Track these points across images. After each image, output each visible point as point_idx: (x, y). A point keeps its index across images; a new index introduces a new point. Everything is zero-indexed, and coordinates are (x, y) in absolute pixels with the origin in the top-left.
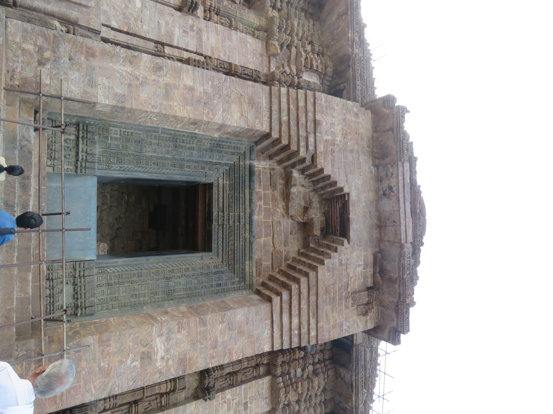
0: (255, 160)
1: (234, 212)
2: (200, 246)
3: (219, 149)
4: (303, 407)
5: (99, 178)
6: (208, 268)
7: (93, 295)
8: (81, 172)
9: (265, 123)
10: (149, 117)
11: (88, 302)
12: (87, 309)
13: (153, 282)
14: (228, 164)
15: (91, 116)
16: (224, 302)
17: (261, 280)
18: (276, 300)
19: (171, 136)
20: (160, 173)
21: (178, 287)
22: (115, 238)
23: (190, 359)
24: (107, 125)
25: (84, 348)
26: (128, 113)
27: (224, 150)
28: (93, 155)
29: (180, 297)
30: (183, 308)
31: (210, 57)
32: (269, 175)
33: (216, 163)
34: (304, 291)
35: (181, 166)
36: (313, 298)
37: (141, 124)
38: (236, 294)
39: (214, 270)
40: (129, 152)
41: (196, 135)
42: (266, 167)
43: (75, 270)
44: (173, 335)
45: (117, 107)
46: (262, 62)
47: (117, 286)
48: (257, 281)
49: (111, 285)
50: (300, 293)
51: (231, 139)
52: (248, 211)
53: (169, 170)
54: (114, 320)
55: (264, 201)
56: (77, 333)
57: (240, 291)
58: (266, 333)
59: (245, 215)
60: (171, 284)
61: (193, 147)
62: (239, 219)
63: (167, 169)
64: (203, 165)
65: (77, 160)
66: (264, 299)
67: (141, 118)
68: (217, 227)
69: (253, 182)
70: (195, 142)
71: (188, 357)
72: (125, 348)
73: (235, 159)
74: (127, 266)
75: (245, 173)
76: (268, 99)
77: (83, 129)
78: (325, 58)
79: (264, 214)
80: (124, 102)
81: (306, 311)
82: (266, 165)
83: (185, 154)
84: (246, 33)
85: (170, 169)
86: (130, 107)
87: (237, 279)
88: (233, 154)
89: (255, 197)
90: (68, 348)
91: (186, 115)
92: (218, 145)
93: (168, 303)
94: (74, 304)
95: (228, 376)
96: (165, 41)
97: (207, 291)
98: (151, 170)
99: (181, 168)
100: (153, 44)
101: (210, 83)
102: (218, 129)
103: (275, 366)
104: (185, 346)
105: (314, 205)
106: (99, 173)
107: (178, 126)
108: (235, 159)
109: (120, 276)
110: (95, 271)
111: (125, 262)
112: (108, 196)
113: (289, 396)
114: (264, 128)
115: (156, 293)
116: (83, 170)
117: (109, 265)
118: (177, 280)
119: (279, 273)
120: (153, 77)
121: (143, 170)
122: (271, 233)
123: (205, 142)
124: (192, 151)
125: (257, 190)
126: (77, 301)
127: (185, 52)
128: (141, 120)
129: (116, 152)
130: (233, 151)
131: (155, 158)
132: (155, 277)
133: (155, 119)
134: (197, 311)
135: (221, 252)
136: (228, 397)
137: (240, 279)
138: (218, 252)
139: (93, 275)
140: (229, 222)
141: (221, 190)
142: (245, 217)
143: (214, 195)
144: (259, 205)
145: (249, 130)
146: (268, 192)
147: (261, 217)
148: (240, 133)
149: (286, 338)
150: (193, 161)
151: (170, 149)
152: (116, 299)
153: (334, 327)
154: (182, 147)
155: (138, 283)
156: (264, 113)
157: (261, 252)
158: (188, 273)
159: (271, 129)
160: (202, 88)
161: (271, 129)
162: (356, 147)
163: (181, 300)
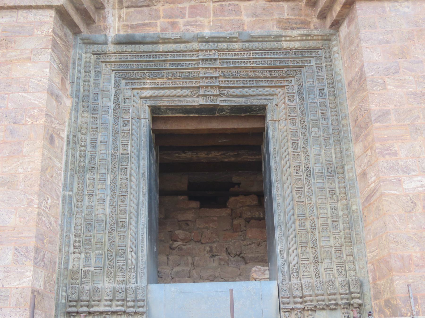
0: (106, 35)
1: (198, 69)
3: (91, 96)
5: (150, 281)
6: (292, 110)
7: (332, 282)
8: (143, 307)
9: (38, 17)
10: (47, 210)
11: (342, 289)
12: (352, 290)
13: (314, 196)
14: (116, 82)
15: (53, 296)
16: (351, 82)
17: (315, 20)
19: (76, 177)
20: (138, 191)
21: (323, 158)
22: (243, 257)
24: (66, 273)
25: (411, 292)
26: (43, 243)
27: (92, 89)
28: (115, 291)
29: (339, 155)
32: (132, 10)
33: (117, 102)
35: (125, 158)
37: (60, 222)
38: (336, 63)
39: (297, 100)
40: (107, 240)
41: (71, 137)
42: (117, 15)
43: (293, 309)
44: (401, 163)
45: (36, 258)
47: (318, 249)
48: (316, 28)
49: (317, 258)
51: (73, 78)
52: (196, 46)
53: (132, 178)
54: (370, 252)
55: (177, 17)
56: (388, 303)
57: (333, 57)
58: (406, 10)
59: (202, 51)
60: (317, 168)
61: (92, 140)
62: (211, 60)
63: (131, 181)
64: (121, 123)
65: (124, 312)
66: (347, 14)
67: (50, 223)
68: (224, 98)
69: (144, 37)
70: (83, 137)
72: (415, 235)
73: (106, 70)
74: (287, 236)
75: (129, 52)
77: (75, 306)
79: (200, 16)
80: (27, 249)
82: (113, 15)
85: (131, 175)
86: (34, 239)
87: (313, 62)
88: (98, 73)
89: (171, 34)
90: (409, 314)
91: (38, 153)
92: (85, 98)
93: (348, 172)
94: (344, 308)
97: (331, 112)
98: (133, 205)
99: (127, 158)
102: (58, 98)
106: (143, 281)
107: (59, 165)
108: (106, 70)
109: (304, 246)
110: (294, 281)
111: (281, 239)
112: (176, 269)
114: (48, 19)
115: (332, 192)
116: (139, 304)
117: (286, 263)
118: (312, 159)
121: (134, 217)
122: (234, 5)
123: (82, 122)
124: (99, 142)
125: (159, 30)
126: (340, 305)
128: (54, 224)
129: (109, 259)
130: (92, 74)
131: (114, 200)
132: (307, 194)
133: (49, 201)
135: (267, 89)
137: (313, 57)
138: (266, 95)
139: (301, 284)
140: (216, 78)
141: (162, 92)
142: (206, 51)
143: (170, 104)
144: (184, 26)
145: (55, 46)
146: (161, 11)
147: (206, 21)
148: (61, 63)
150: (115, 140)
151: (97, 177)
152: (339, 251)
154: (92, 158)
155: (315, 219)
156: (22, 20)
157: (267, 20)
158: (301, 143)
159: (49, 7)
161: (49, 7)
163: (344, 152)
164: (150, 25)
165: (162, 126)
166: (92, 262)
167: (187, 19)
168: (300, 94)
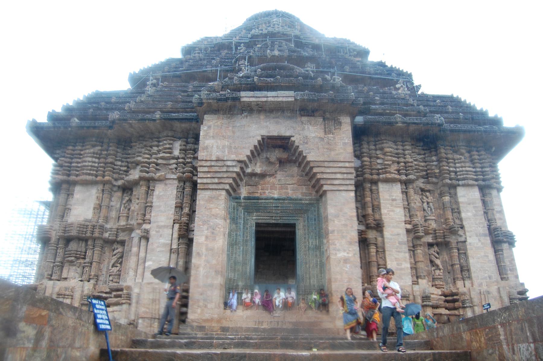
2: (293, 230)
4: (402, 160)
17: (314, 193)
18: (325, 188)
21: (314, 244)
23: (351, 239)
30: (325, 241)
31: (174, 220)
33: (244, 220)
34: (322, 170)
35: (247, 241)
36: (326, 164)
39: (306, 222)
44: (337, 248)
46: (170, 184)
50: (322, 173)
52: (272, 201)
64: (245, 228)
68: (281, 220)
70: (233, 233)
71: (349, 240)
73: (240, 209)
76: (206, 191)
78: (161, 136)
81: (334, 169)
83: (240, 239)
84: (153, 195)
88: (237, 210)
89: (263, 196)
91: (221, 240)
95: (374, 210)
96: (169, 248)
100: (172, 255)
101: (201, 226)
103: (372, 179)
104: (344, 242)
105: (268, 156)
113: (392, 171)
115: (316, 255)
118: (310, 243)
119: (310, 181)
120: (203, 257)
127: (174, 236)
130: (236, 210)
134: (327, 234)
136: (386, 212)
138: (295, 220)
141: (260, 217)
147: (276, 192)
149: (348, 182)
150: (244, 234)
153: (345, 150)
154: (236, 241)
158: (307, 238)
159: (223, 189)
160: (205, 231)
161: (223, 189)
162: (230, 128)
164: (256, 192)
165: (259, 229)
166: (236, 276)
167: (269, 191)
168: (308, 220)
